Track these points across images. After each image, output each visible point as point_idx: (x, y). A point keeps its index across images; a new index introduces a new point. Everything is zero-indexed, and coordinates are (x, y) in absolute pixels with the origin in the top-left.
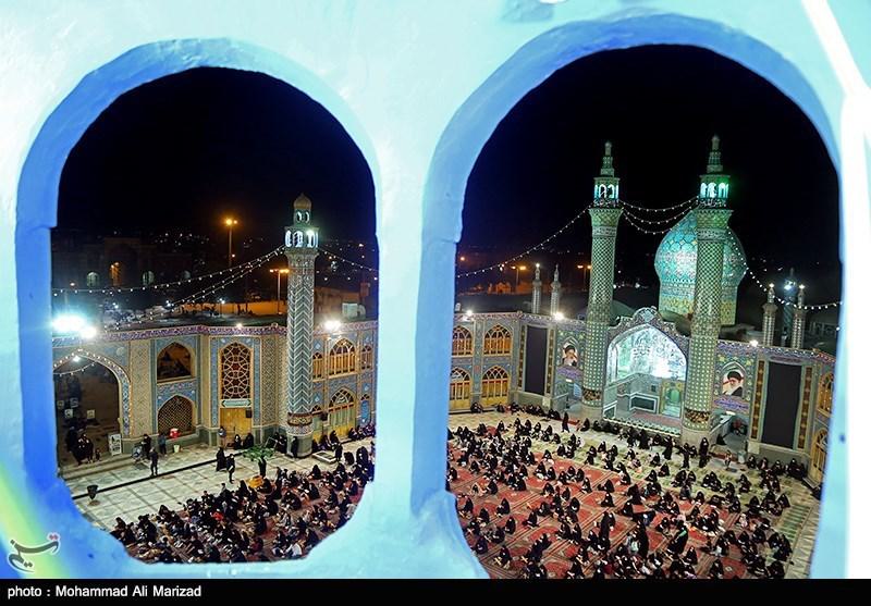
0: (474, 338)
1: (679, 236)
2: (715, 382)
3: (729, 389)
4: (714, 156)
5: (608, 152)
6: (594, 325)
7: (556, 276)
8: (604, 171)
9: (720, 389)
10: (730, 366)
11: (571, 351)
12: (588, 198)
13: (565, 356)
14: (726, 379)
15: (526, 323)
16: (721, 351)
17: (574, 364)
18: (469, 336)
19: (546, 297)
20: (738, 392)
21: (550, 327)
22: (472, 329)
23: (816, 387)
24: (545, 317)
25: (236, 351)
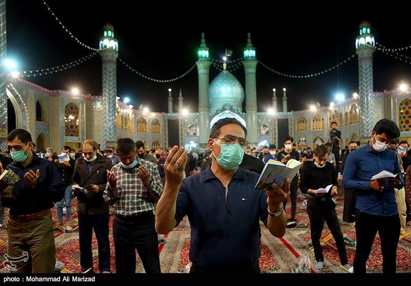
0: (147, 123)
2: (258, 130)
3: (263, 132)
4: (249, 40)
5: (203, 37)
6: (202, 113)
7: (181, 94)
8: (202, 45)
9: (260, 133)
10: (263, 122)
11: (192, 128)
12: (196, 58)
13: (189, 130)
14: (262, 128)
15: (167, 118)
16: (259, 117)
17: (194, 134)
18: (146, 123)
19: (175, 102)
20: (267, 133)
21: (180, 118)
22: (147, 119)
23: (294, 124)
24: (177, 114)
25: (72, 108)
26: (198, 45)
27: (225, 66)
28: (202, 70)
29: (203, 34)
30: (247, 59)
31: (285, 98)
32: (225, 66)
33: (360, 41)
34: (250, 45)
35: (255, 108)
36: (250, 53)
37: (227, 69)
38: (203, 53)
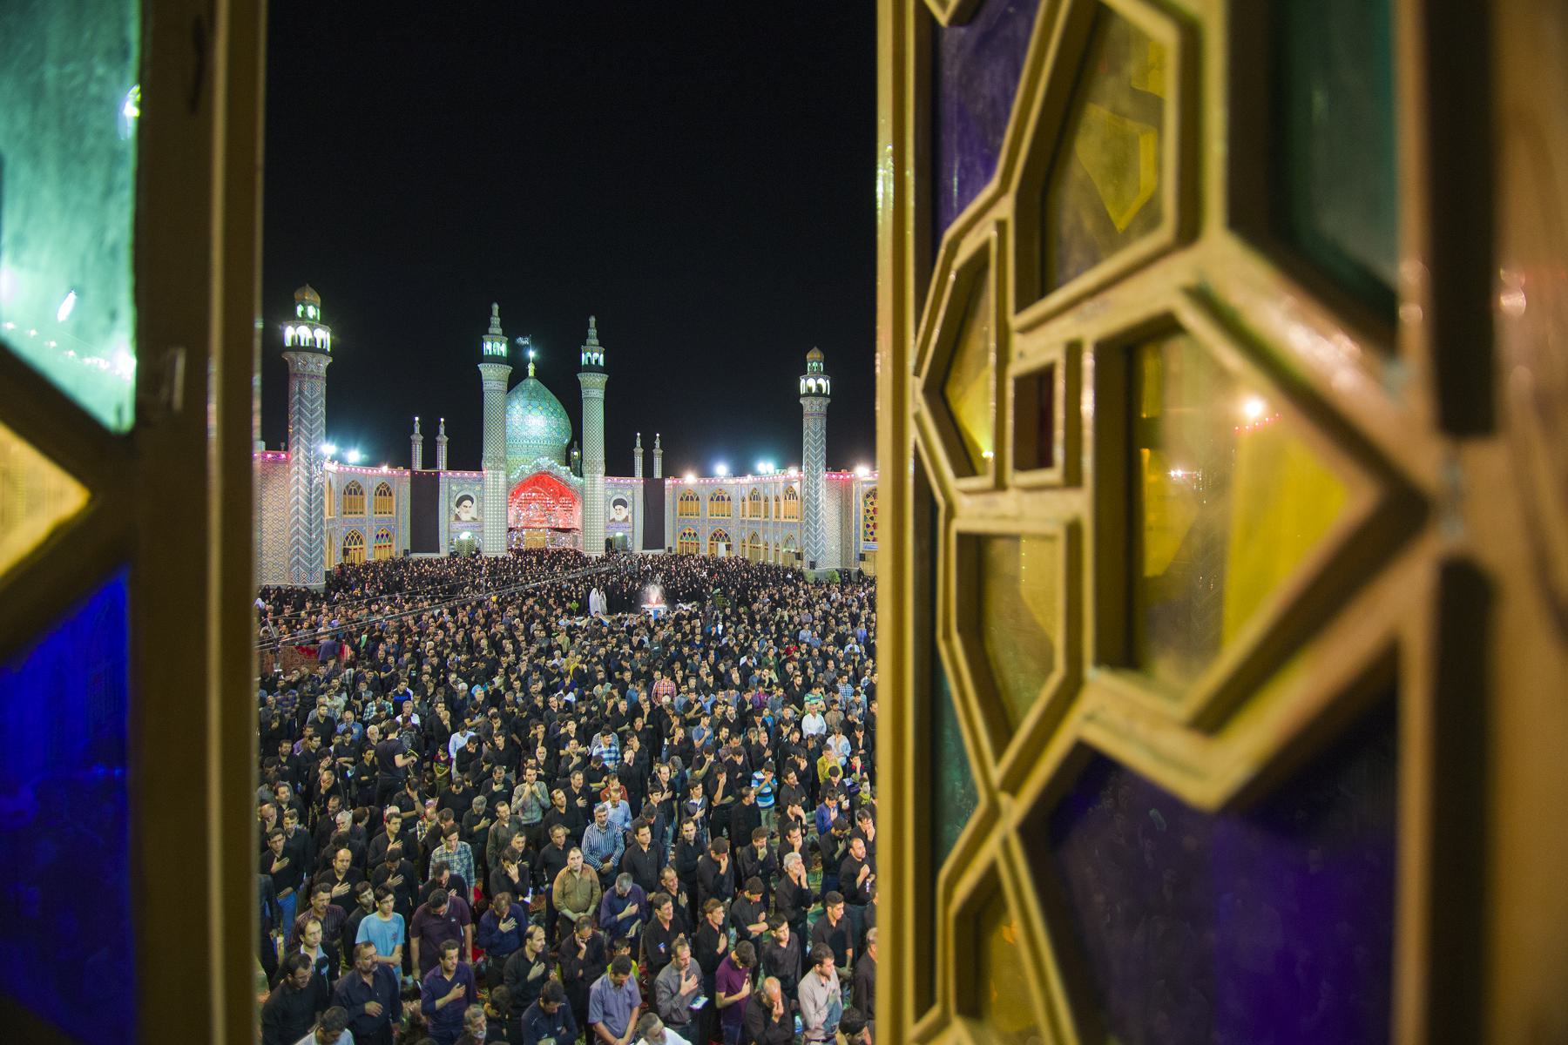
1: (524, 402)
4: (593, 332)
8: (491, 330)
11: (467, 503)
26: (484, 328)
27: (531, 367)
28: (493, 377)
29: (496, 307)
30: (592, 368)
31: (658, 452)
32: (531, 367)
33: (808, 383)
34: (596, 342)
35: (602, 468)
36: (593, 355)
37: (537, 375)
38: (495, 346)
